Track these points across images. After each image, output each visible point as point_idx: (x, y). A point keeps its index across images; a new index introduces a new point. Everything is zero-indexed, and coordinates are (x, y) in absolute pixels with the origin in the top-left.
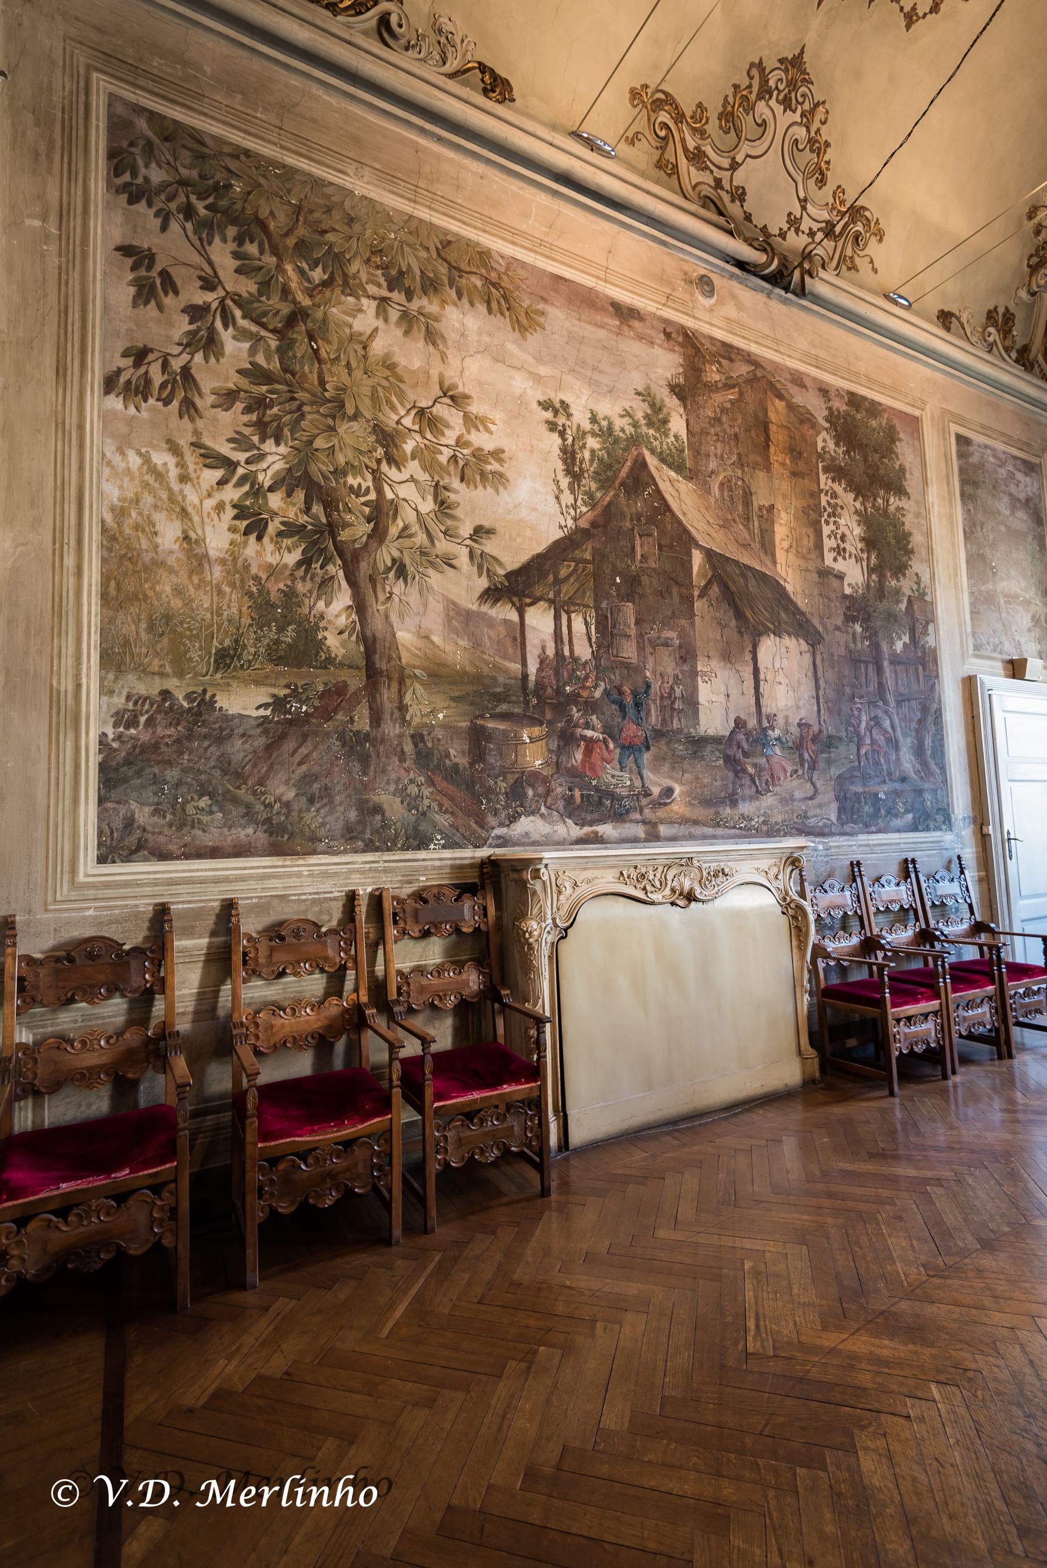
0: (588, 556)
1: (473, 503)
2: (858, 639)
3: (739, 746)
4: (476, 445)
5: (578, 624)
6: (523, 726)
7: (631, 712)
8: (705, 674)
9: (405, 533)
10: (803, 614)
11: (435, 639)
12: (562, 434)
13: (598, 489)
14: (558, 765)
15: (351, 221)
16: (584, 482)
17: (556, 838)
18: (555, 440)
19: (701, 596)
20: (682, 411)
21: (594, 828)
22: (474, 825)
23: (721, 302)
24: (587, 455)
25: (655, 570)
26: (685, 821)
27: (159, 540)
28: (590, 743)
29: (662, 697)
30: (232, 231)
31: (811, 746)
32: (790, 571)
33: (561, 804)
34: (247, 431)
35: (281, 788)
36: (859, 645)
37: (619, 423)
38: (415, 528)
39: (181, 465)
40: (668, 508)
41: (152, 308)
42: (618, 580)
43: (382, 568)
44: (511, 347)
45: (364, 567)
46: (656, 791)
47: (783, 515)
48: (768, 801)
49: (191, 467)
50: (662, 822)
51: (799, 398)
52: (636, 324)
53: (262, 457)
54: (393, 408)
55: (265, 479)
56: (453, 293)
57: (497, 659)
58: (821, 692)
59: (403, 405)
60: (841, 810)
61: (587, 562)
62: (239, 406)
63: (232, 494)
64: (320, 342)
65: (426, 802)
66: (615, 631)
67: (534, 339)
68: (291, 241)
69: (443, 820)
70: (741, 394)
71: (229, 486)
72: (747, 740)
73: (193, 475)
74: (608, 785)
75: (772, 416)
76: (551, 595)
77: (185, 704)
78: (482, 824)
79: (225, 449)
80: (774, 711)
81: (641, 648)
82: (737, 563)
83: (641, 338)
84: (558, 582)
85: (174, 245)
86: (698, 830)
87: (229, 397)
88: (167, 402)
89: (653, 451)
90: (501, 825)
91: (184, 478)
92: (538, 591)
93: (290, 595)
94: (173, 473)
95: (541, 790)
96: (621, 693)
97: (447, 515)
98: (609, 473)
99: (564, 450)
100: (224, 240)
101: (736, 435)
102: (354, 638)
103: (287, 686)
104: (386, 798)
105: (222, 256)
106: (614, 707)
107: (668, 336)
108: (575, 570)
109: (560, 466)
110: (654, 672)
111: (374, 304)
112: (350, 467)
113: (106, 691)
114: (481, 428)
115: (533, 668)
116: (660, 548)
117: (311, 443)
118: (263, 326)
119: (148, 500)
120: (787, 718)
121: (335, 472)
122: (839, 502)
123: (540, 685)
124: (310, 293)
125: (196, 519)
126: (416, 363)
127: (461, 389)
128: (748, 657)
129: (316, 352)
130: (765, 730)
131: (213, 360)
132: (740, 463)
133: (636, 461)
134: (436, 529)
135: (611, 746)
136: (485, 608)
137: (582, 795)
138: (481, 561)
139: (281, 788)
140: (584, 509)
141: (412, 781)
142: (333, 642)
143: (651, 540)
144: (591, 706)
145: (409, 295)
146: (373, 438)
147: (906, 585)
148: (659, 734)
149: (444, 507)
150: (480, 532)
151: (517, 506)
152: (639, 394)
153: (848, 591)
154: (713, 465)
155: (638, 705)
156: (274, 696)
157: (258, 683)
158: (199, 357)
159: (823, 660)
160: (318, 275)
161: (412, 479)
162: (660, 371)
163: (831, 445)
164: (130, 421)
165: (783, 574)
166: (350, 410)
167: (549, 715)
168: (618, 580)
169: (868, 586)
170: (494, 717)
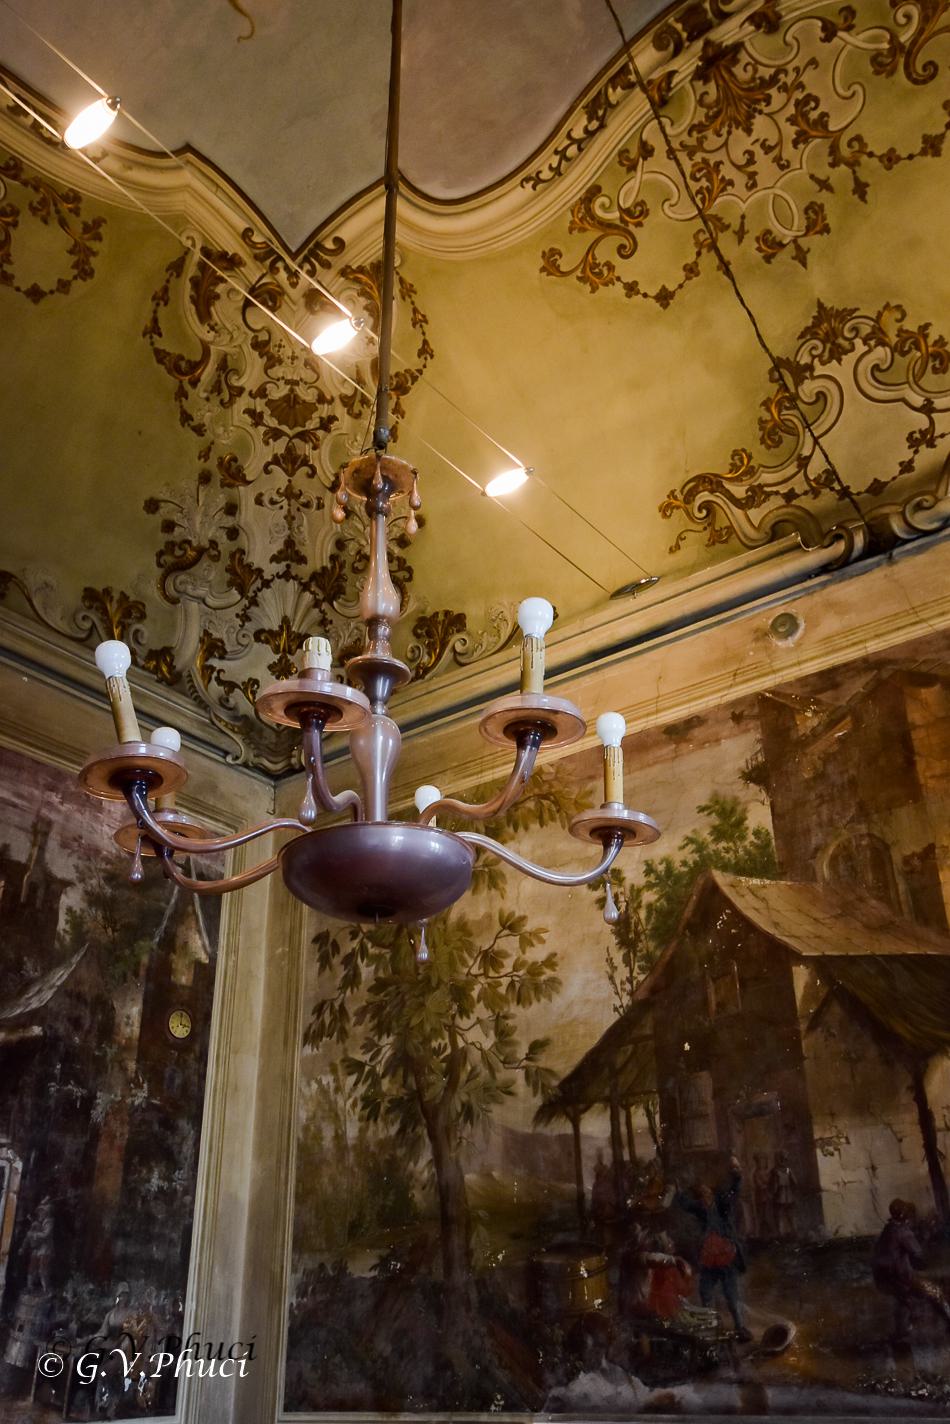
0: (648, 1031)
1: (529, 1020)
4: (530, 961)
5: (639, 1119)
8: (827, 1142)
9: (473, 1075)
13: (656, 948)
16: (640, 945)
19: (811, 1028)
20: (763, 795)
23: (813, 623)
24: (643, 914)
28: (659, 1267)
34: (371, 1035)
39: (336, 1080)
40: (750, 926)
42: (687, 1047)
43: (454, 1116)
45: (441, 1120)
46: (758, 1333)
49: (341, 1078)
54: (464, 963)
55: (380, 1069)
56: (511, 830)
61: (647, 1038)
62: (368, 1016)
63: (362, 1089)
71: (360, 1085)
77: (331, 1273)
83: (701, 745)
84: (615, 1073)
89: (725, 868)
94: (332, 1085)
95: (602, 1337)
96: (698, 1195)
98: (670, 922)
107: (737, 718)
108: (634, 1053)
109: (614, 940)
110: (743, 1157)
113: (294, 1270)
114: (535, 942)
115: (588, 1185)
117: (408, 1024)
118: (384, 947)
119: (320, 1114)
125: (342, 1118)
126: (482, 911)
127: (517, 915)
133: (704, 889)
134: (495, 1060)
135: (689, 1271)
136: (541, 1129)
138: (534, 1078)
142: (417, 1195)
143: (728, 979)
144: (659, 1220)
148: (756, 1246)
149: (503, 1034)
150: (537, 1047)
151: (570, 1006)
152: (702, 809)
155: (723, 1208)
157: (372, 1246)
161: (479, 1021)
164: (315, 1058)
166: (434, 984)
168: (687, 1047)
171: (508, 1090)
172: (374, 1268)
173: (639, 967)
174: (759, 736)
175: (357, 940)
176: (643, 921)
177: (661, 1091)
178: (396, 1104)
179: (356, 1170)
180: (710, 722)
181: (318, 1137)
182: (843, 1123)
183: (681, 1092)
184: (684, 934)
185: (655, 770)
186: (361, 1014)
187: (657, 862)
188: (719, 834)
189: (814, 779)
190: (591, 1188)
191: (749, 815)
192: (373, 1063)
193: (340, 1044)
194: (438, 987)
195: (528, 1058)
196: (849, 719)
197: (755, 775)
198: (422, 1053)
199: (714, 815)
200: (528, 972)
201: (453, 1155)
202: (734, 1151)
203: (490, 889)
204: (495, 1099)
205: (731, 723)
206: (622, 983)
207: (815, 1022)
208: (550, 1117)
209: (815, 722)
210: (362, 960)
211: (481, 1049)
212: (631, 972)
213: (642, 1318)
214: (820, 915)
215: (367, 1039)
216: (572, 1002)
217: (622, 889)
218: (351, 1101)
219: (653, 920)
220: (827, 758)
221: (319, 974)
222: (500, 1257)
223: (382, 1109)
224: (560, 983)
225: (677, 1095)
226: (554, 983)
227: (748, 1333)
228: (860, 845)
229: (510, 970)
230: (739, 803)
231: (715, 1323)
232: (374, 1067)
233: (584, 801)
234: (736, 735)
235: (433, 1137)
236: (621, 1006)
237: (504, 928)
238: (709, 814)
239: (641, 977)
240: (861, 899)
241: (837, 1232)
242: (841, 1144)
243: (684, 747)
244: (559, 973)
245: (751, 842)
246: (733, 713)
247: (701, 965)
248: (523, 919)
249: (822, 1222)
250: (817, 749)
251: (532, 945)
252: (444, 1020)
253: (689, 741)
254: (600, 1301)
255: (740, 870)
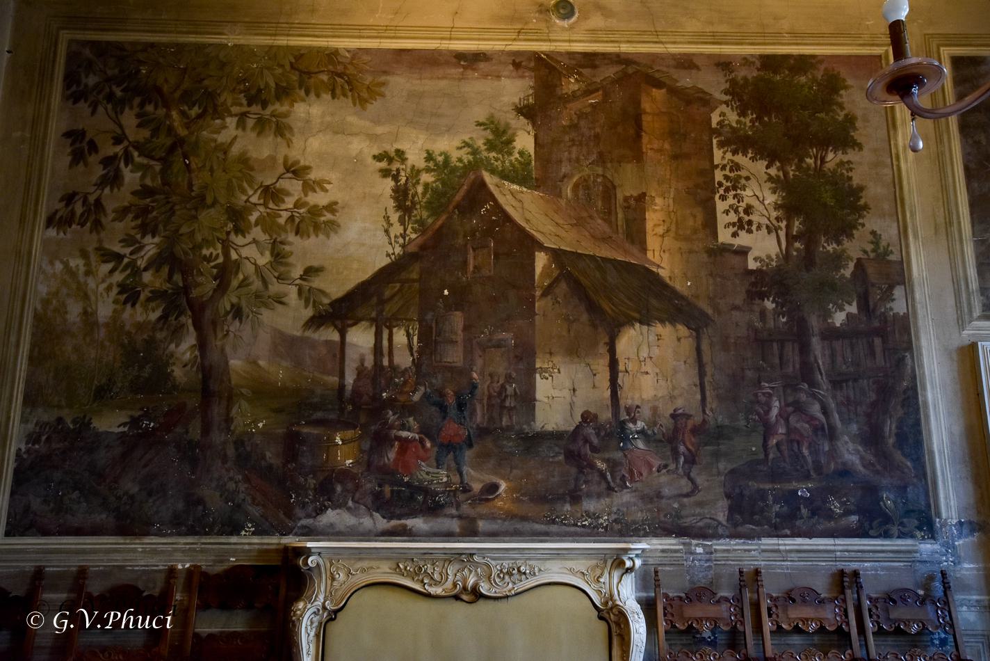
0: (415, 276)
1: (305, 250)
2: (770, 316)
3: (586, 441)
4: (312, 203)
5: (400, 337)
6: (337, 430)
7: (453, 412)
8: (543, 370)
9: (244, 283)
10: (682, 298)
11: (261, 363)
12: (396, 178)
13: (429, 217)
14: (369, 465)
15: (223, 65)
16: (415, 212)
17: (361, 529)
18: (390, 183)
19: (544, 295)
20: (530, 128)
21: (403, 521)
22: (281, 515)
24: (420, 189)
25: (489, 278)
26: (511, 516)
27: (68, 316)
28: (405, 442)
29: (490, 397)
30: (137, 100)
31: (680, 438)
32: (666, 256)
33: (369, 500)
34: (133, 232)
35: (129, 486)
36: (771, 324)
37: (455, 155)
38: (253, 278)
39: (87, 264)
40: (507, 218)
41: (81, 167)
42: (446, 292)
43: (222, 312)
44: (351, 119)
45: (208, 314)
47: (659, 201)
48: (625, 497)
49: (94, 264)
50: (482, 517)
51: (686, 81)
52: (482, 65)
53: (141, 248)
54: (244, 191)
55: (141, 263)
56: (302, 93)
57: (316, 374)
58: (707, 379)
59: (251, 186)
60: (732, 510)
61: (414, 281)
62: (130, 216)
63: (118, 277)
64: (191, 158)
65: (242, 496)
66: (439, 339)
67: (374, 107)
68: (177, 94)
69: (255, 511)
70: (606, 95)
71: (117, 273)
72: (598, 435)
73: (94, 269)
74: (420, 481)
75: (646, 105)
76: (374, 314)
77: (71, 426)
78: (290, 514)
79: (117, 248)
80: (637, 402)
81: (468, 352)
82: (592, 258)
83: (485, 76)
84: (382, 302)
85: (97, 123)
86: (527, 526)
87: (122, 213)
88: (82, 225)
89: (493, 171)
90: (308, 516)
91: (88, 273)
92: (361, 312)
93: (151, 343)
94: (82, 269)
95: (350, 486)
96: (442, 395)
97: (281, 264)
98: (443, 201)
99: (396, 190)
100: (131, 108)
101: (597, 136)
102: (195, 369)
103: (142, 409)
104: (209, 493)
105: (129, 119)
106: (433, 408)
107: (517, 65)
108: (400, 290)
109: (391, 204)
110: (482, 374)
111: (235, 120)
112: (207, 243)
114: (318, 190)
115: (350, 379)
116: (496, 255)
117: (177, 231)
118: (152, 158)
120: (655, 410)
121: (192, 249)
122: (743, 173)
123: (355, 391)
124: (187, 126)
125: (93, 298)
126: (266, 153)
127: (302, 163)
128: (603, 349)
129: (188, 166)
130: (624, 422)
131: (116, 190)
132: (602, 159)
135: (428, 445)
136: (309, 333)
137: (392, 492)
138: (307, 295)
139: (129, 486)
140: (414, 236)
141: (231, 479)
142: (178, 372)
143: (485, 251)
144: (409, 409)
145: (264, 105)
146: (226, 217)
147: (854, 248)
148: (483, 432)
150: (310, 272)
151: (346, 245)
152: (479, 124)
153: (752, 265)
154: (565, 168)
155: (461, 406)
156: (131, 417)
157: (121, 408)
158: (107, 191)
159: (712, 345)
160: (195, 111)
161: (255, 241)
162: (505, 99)
163: (733, 117)
165: (657, 260)
166: (209, 200)
167: (363, 419)
168: (446, 292)
169: (787, 256)
170: (309, 423)
171: (280, 300)
172: (124, 424)
173: (412, 228)
174: (532, 84)
175: (121, 146)
176: (420, 196)
177: (421, 321)
178: (157, 295)
179: (107, 344)
180: (494, 61)
181: (62, 310)
182: (557, 359)
183: (437, 323)
184: (453, 212)
185: (443, 83)
186: (122, 213)
187: (437, 153)
188: (491, 146)
189: (570, 127)
190: (352, 382)
191: (516, 138)
192: (134, 257)
193: (94, 233)
194: (213, 205)
195: (301, 278)
196: (600, 92)
197: (525, 111)
198: (191, 257)
199: (488, 131)
200: (309, 212)
201: (219, 343)
202: (475, 368)
203: (276, 136)
204: (266, 306)
205: (511, 67)
206: (396, 237)
207: (547, 292)
208: (318, 327)
209: (576, 87)
210: (126, 165)
211: (255, 264)
212: (405, 230)
213: (387, 474)
214: (561, 222)
215: (127, 235)
216: (349, 243)
217: (404, 167)
218: (104, 285)
219: (428, 196)
220: (581, 115)
221: (71, 166)
222: (260, 425)
223: (142, 297)
224: (339, 226)
225: (434, 325)
226: (333, 226)
227: (470, 487)
228: (596, 181)
229: (291, 206)
230: (510, 128)
231: (445, 479)
232: (135, 261)
233: (377, 89)
234: (514, 78)
235: (198, 326)
236: (393, 254)
237: (288, 171)
238: (485, 129)
239: (414, 236)
240: (591, 217)
241: (543, 427)
242: (554, 373)
243: (469, 73)
244: (339, 218)
245: (516, 159)
246: (514, 60)
247: (465, 236)
248: (307, 168)
249: (534, 420)
250: (575, 106)
251: (315, 192)
252: (219, 235)
253: (474, 70)
254: (351, 461)
255: (504, 176)
